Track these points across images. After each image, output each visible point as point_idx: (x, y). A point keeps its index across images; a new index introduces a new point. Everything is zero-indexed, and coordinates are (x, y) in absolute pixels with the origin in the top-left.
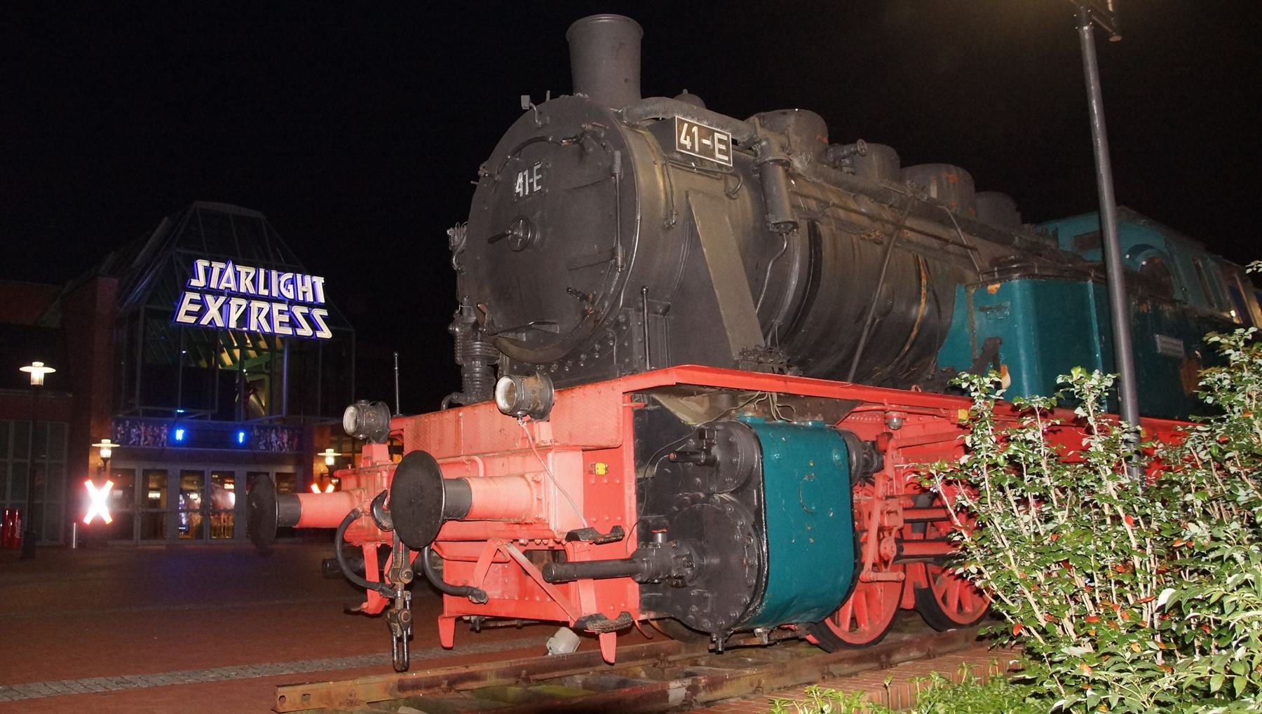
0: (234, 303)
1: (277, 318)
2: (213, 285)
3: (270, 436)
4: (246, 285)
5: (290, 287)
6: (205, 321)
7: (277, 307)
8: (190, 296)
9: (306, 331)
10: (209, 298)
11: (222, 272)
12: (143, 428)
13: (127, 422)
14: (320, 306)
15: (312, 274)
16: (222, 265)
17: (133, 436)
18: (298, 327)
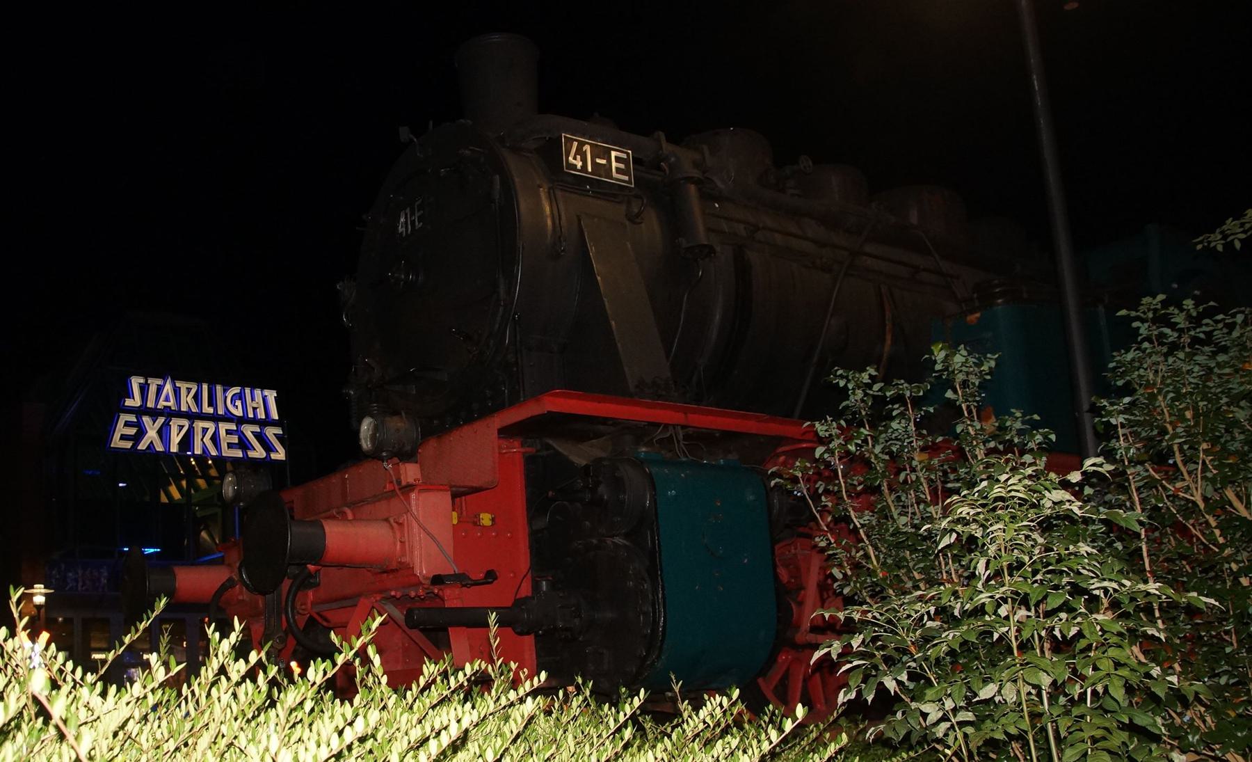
0: (174, 423)
1: (225, 439)
2: (150, 404)
4: (187, 402)
5: (238, 403)
6: (142, 446)
7: (223, 427)
8: (124, 418)
9: (258, 452)
11: (160, 389)
12: (80, 572)
13: (63, 566)
14: (274, 423)
15: (262, 388)
16: (160, 382)
18: (249, 449)
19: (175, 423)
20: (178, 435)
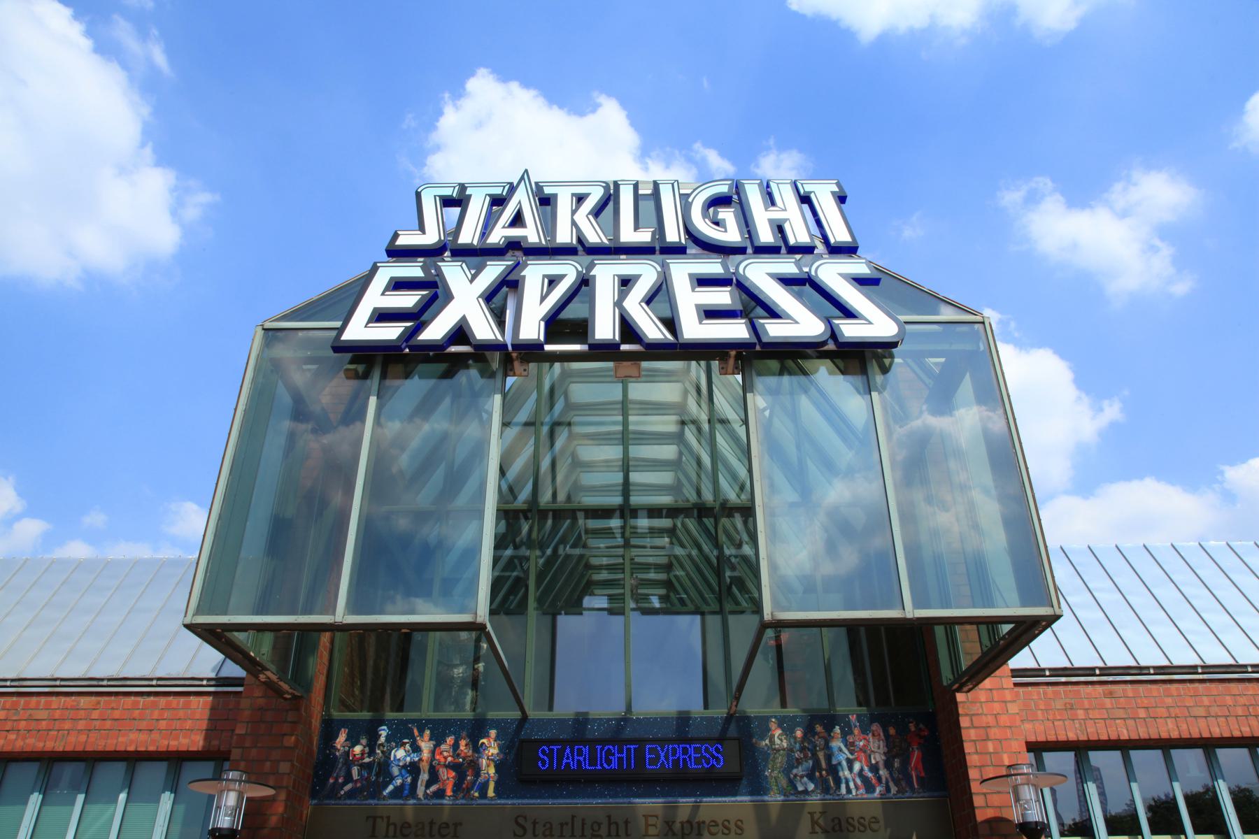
1: (688, 300)
6: (436, 331)
7: (681, 271)
19: (534, 273)
20: (543, 299)
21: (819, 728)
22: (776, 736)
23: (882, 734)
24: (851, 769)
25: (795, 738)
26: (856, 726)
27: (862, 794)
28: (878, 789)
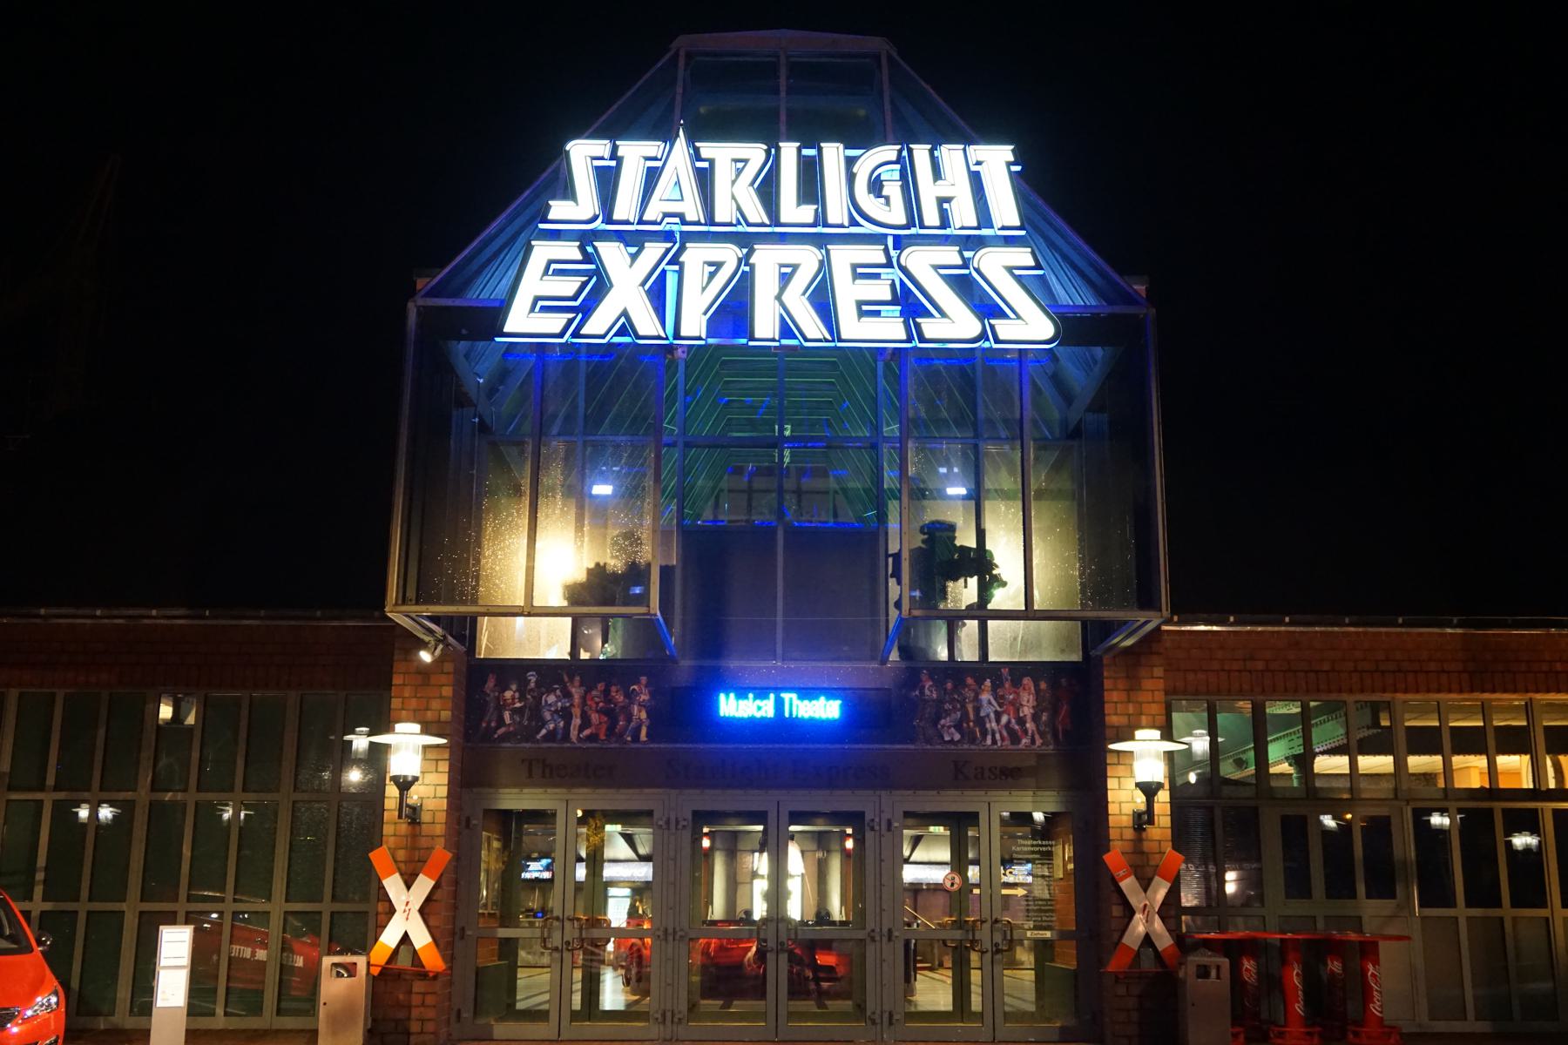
1: (847, 293)
3: (977, 699)
7: (843, 257)
10: (612, 254)
11: (652, 177)
16: (653, 148)
17: (547, 716)
20: (704, 289)
21: (970, 681)
22: (927, 687)
23: (1033, 688)
24: (998, 721)
25: (945, 689)
26: (1007, 680)
27: (1007, 745)
28: (1024, 741)
